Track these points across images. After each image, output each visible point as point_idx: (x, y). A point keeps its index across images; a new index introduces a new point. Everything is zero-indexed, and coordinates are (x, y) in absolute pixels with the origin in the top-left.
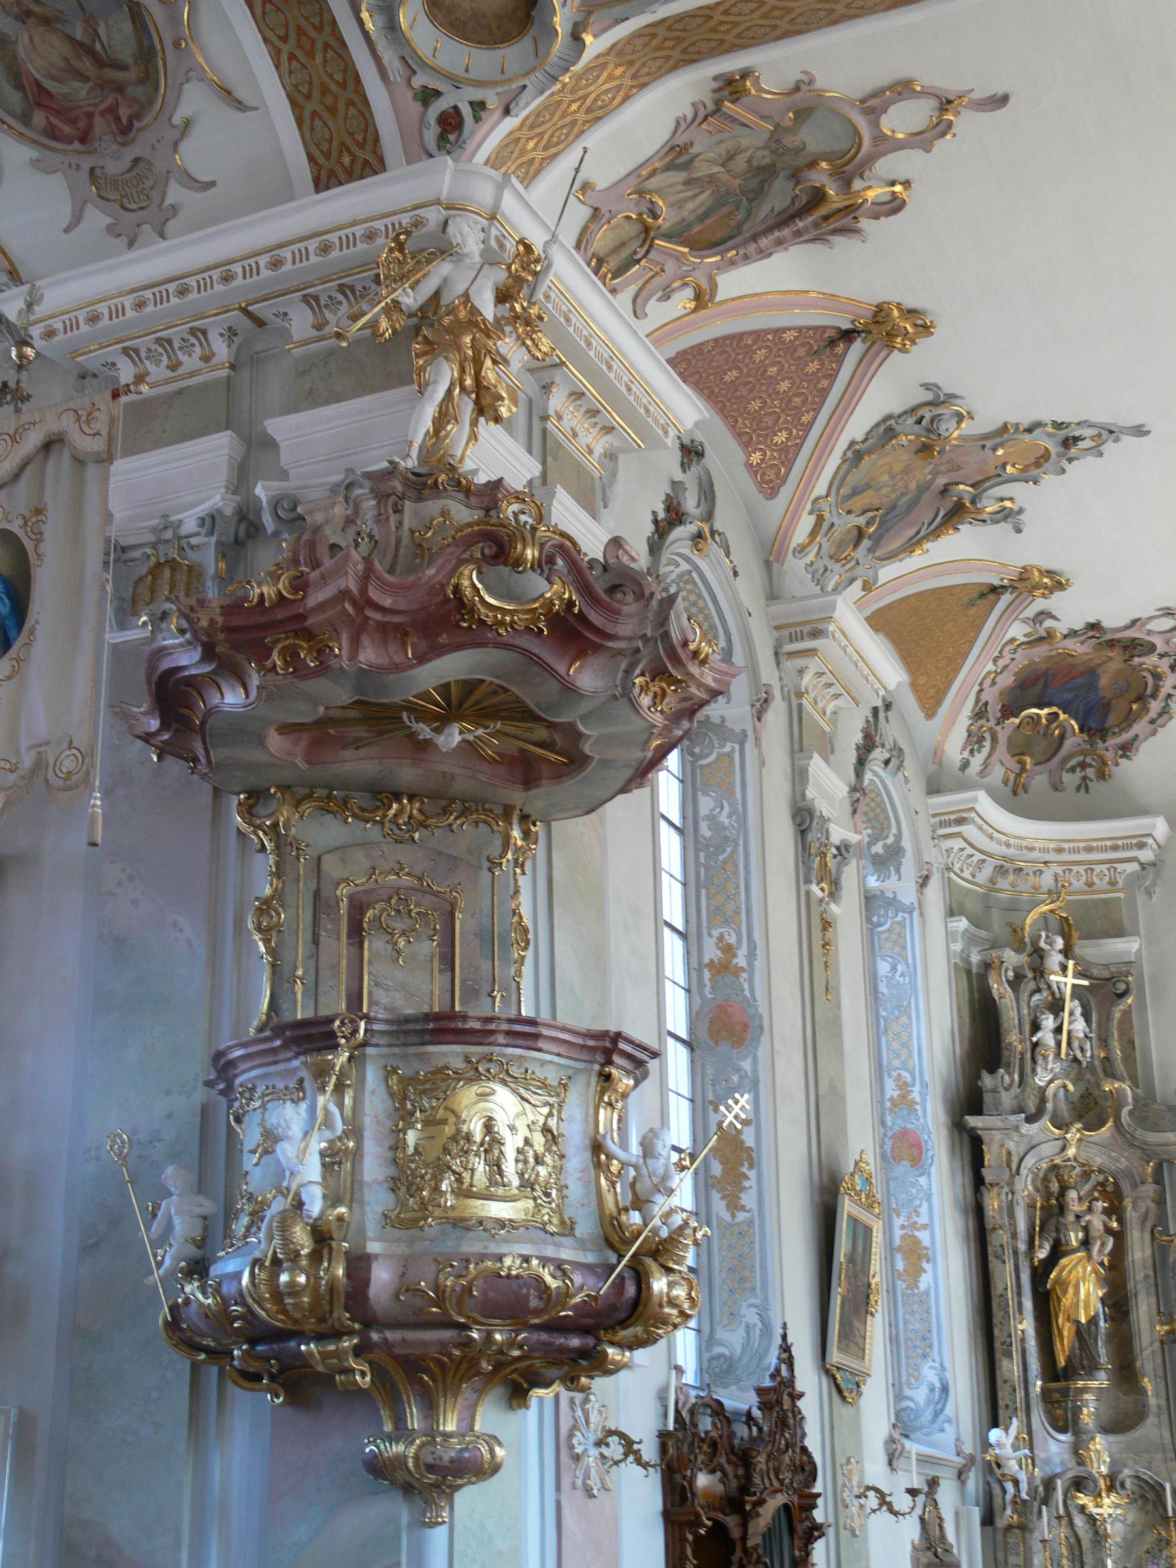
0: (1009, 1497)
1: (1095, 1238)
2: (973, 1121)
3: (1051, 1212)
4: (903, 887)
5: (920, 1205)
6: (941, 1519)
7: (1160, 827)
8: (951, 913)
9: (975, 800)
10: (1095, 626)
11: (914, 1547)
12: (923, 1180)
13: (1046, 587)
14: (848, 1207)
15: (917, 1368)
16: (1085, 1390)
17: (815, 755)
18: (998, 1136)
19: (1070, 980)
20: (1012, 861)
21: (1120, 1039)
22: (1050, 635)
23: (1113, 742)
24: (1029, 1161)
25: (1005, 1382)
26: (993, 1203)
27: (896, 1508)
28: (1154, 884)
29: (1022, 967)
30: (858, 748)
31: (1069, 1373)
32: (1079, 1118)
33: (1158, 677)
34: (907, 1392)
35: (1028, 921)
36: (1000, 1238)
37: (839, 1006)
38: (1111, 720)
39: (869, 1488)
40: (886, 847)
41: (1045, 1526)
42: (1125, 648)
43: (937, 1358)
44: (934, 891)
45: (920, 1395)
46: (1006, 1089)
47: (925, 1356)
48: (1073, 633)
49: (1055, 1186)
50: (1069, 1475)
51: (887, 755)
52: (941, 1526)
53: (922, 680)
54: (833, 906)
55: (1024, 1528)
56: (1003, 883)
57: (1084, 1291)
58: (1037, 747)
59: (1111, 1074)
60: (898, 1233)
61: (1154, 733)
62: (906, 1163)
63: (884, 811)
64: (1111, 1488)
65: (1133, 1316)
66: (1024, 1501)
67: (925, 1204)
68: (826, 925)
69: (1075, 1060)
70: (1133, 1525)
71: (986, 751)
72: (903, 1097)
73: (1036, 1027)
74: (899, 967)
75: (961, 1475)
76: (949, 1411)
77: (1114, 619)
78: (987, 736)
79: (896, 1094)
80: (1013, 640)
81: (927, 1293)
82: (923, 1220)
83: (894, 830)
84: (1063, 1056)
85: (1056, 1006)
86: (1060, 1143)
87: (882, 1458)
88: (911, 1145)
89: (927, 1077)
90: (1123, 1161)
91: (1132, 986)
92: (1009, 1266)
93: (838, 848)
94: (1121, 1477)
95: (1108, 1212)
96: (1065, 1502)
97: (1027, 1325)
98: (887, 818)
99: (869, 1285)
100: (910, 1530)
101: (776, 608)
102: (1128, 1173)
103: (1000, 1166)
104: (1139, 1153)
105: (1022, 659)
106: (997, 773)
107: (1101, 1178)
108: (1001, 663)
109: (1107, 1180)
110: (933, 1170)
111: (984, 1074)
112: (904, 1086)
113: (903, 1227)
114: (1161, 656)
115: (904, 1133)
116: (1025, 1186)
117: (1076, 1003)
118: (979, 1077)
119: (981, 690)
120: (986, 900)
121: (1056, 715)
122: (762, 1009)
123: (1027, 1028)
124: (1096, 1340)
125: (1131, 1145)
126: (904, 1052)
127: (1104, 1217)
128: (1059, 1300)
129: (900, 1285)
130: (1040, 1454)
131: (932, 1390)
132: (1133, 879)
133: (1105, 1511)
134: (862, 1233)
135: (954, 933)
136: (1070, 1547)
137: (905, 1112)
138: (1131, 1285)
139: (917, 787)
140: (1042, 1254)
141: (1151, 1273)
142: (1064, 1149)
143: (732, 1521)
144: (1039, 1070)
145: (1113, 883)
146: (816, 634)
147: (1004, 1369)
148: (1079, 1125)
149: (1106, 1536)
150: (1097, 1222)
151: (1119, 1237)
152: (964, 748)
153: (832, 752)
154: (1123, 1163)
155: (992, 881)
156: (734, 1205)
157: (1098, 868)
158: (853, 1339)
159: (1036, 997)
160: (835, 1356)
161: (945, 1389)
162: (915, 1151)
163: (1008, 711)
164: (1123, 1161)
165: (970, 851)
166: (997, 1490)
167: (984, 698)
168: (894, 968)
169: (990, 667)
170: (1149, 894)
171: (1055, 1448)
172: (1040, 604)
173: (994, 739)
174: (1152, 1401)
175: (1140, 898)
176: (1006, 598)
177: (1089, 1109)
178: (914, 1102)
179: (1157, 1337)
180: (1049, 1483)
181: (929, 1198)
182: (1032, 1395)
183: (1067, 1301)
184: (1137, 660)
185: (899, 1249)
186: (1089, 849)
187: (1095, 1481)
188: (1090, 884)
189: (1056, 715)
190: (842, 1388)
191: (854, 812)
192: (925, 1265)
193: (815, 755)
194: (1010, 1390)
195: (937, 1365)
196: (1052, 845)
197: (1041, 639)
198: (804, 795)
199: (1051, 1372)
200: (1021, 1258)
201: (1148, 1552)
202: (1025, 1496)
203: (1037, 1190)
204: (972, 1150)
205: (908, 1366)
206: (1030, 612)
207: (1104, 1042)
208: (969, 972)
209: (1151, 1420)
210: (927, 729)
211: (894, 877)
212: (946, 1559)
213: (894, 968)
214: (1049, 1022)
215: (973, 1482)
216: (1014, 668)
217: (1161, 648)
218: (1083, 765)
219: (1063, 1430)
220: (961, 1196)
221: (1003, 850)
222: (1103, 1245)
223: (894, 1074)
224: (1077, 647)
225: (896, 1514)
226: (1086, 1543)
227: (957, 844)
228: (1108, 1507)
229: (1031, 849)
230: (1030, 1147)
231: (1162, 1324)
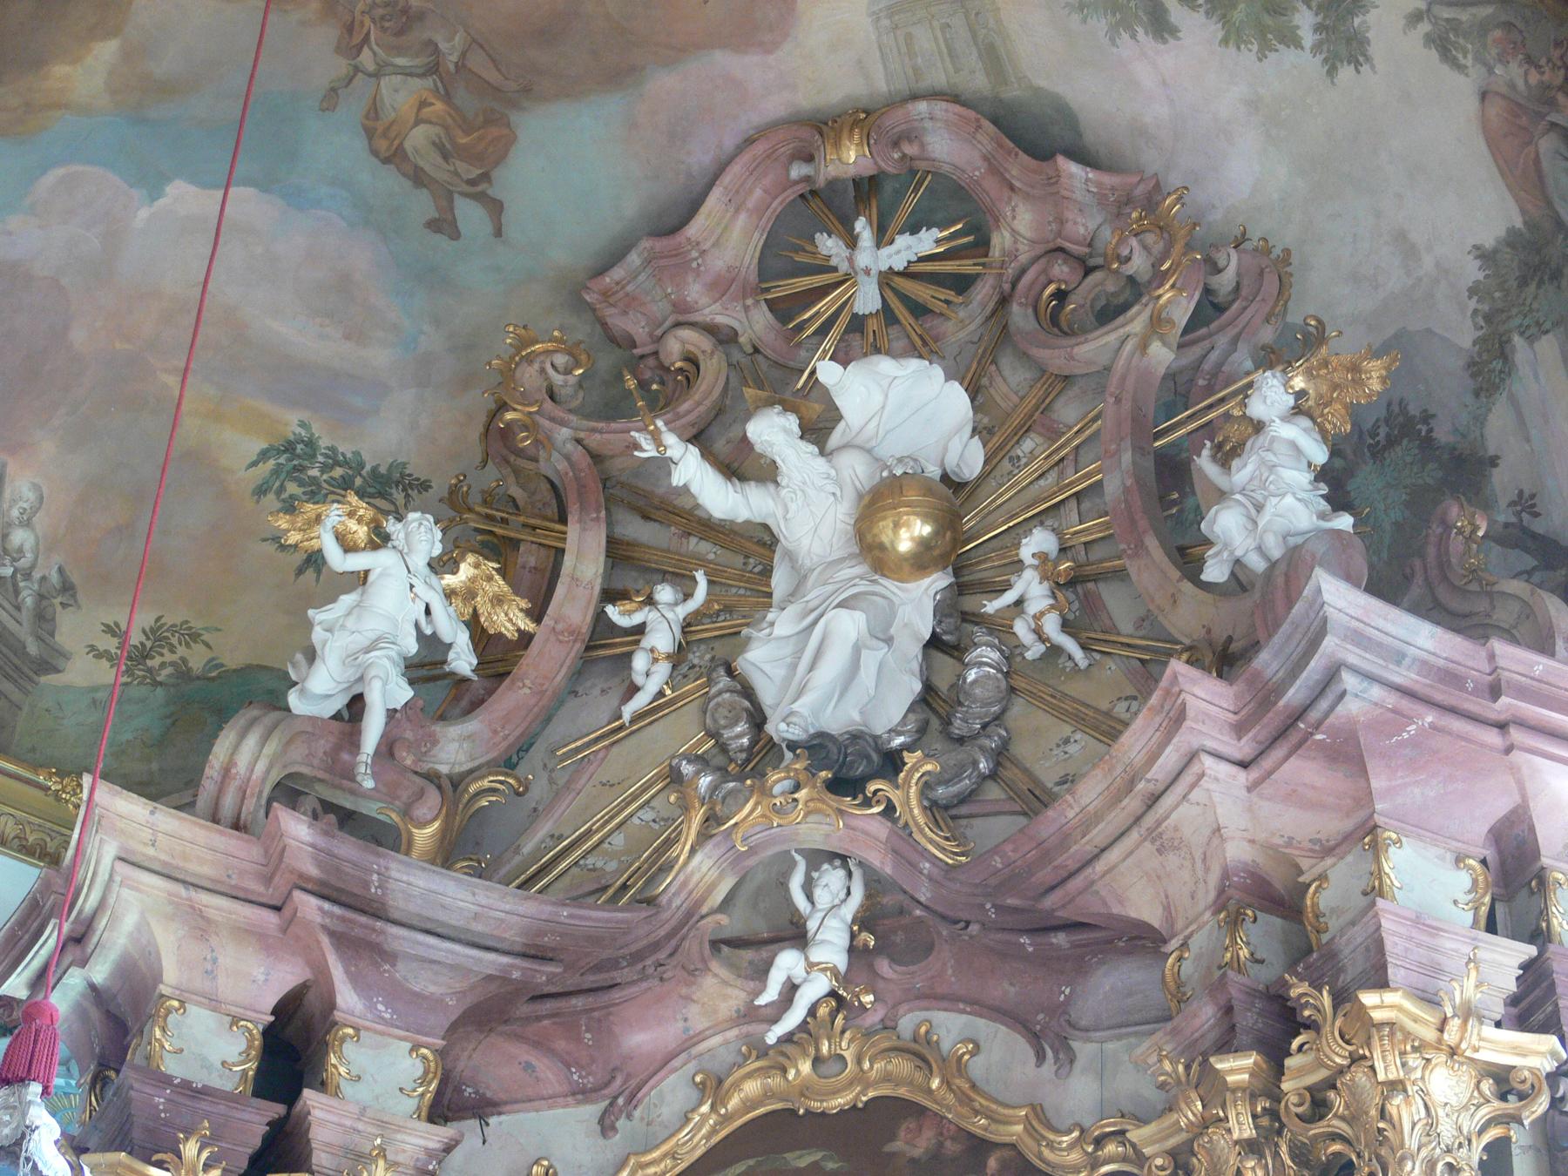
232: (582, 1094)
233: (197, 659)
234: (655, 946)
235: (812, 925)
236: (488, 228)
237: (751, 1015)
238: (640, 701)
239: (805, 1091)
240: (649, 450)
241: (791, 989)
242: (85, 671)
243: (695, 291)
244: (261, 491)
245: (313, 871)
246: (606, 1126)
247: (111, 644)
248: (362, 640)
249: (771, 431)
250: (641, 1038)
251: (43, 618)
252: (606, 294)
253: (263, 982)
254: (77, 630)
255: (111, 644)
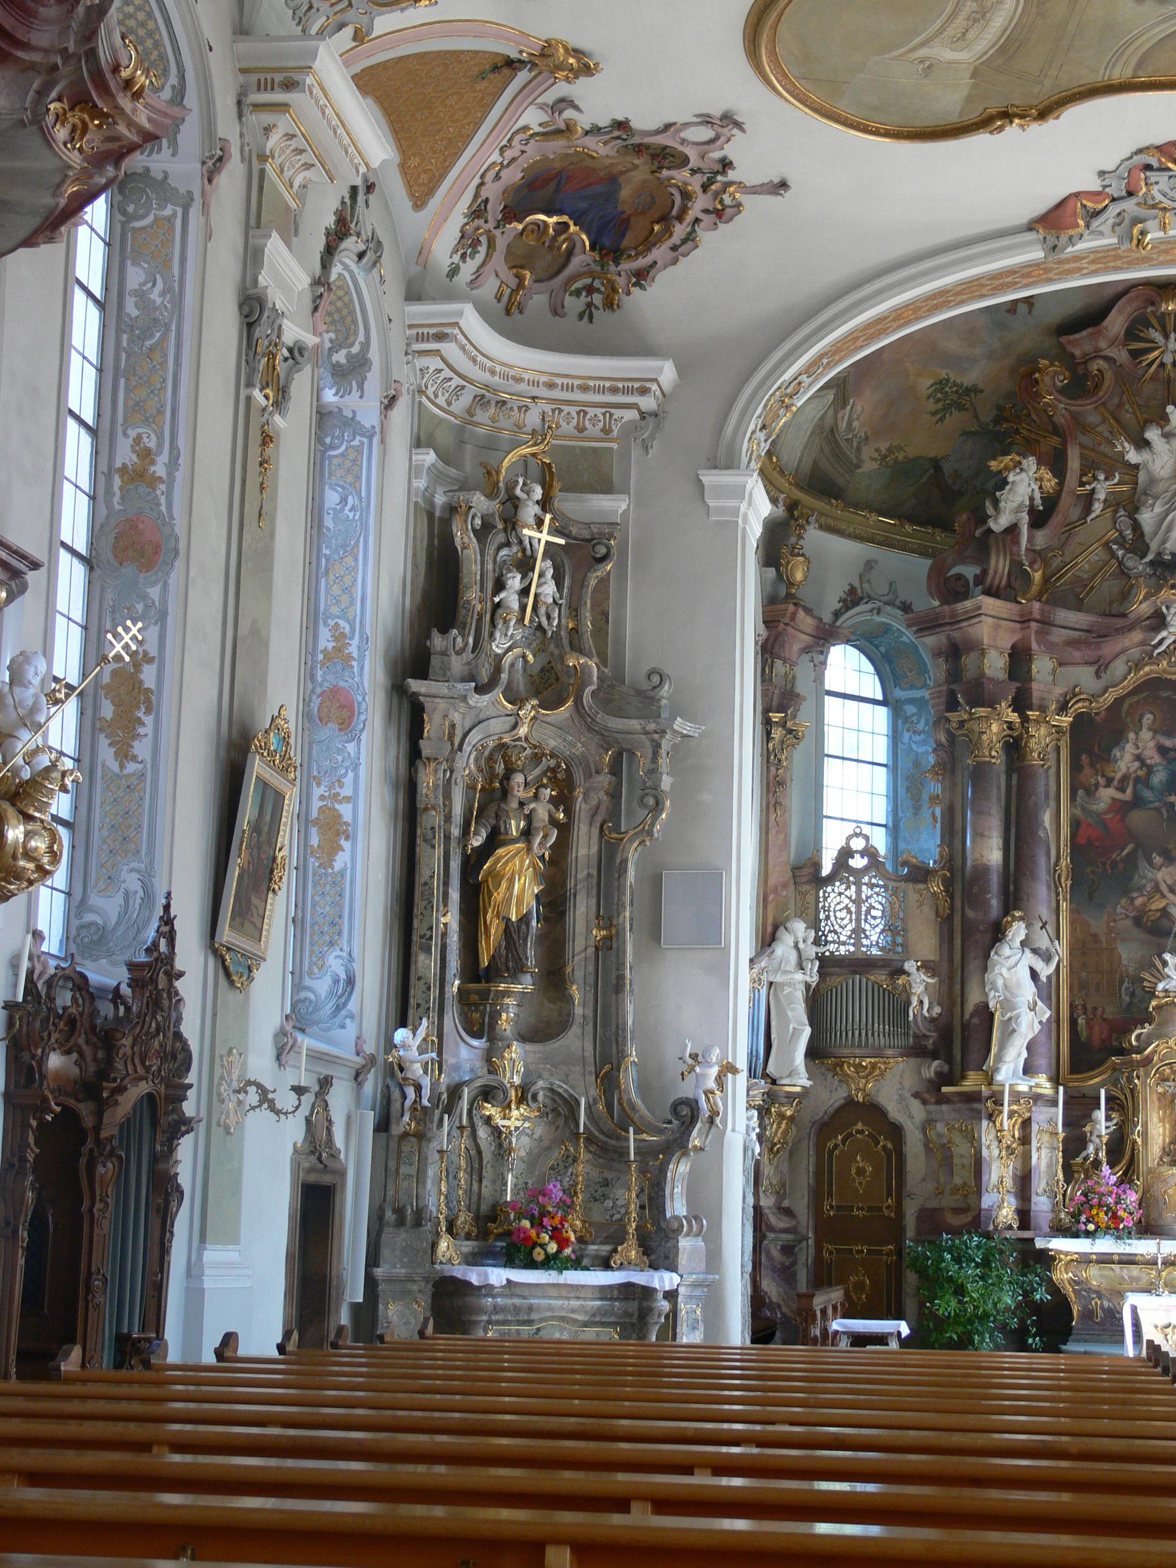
0: (408, 1103)
1: (537, 829)
2: (415, 685)
3: (492, 797)
4: (365, 406)
5: (346, 774)
6: (330, 1122)
7: (667, 373)
8: (418, 443)
9: (460, 313)
10: (622, 125)
11: (296, 1150)
12: (351, 747)
13: (571, 70)
14: (257, 768)
15: (322, 956)
16: (507, 993)
17: (274, 234)
18: (442, 704)
19: (545, 537)
20: (495, 391)
21: (593, 609)
22: (568, 130)
23: (626, 266)
24: (474, 737)
25: (420, 978)
26: (428, 780)
27: (279, 1106)
28: (652, 437)
29: (492, 515)
30: (328, 234)
31: (493, 973)
32: (537, 694)
33: (686, 196)
34: (308, 982)
35: (506, 464)
36: (432, 819)
37: (272, 536)
38: (626, 242)
39: (250, 1083)
40: (349, 357)
41: (444, 1136)
42: (654, 156)
43: (345, 948)
44: (401, 416)
45: (322, 986)
46: (458, 653)
47: (332, 944)
48: (595, 130)
49: (500, 768)
50: (478, 1083)
51: (362, 247)
52: (329, 1130)
53: (413, 162)
54: (277, 418)
55: (421, 1136)
56: (482, 416)
57: (518, 886)
58: (537, 261)
59: (577, 648)
60: (316, 804)
61: (675, 262)
62: (333, 726)
63: (352, 313)
64: (521, 1100)
65: (569, 918)
66: (425, 1108)
67: (351, 775)
68: (267, 439)
69: (540, 627)
70: (541, 1139)
71: (480, 258)
72: (338, 650)
73: (500, 586)
74: (350, 499)
75: (358, 1076)
76: (352, 1006)
77: (645, 120)
78: (483, 239)
79: (330, 645)
80: (525, 128)
81: (342, 873)
82: (347, 791)
83: (361, 337)
84: (527, 622)
85: (525, 565)
86: (512, 720)
87: (269, 1050)
88: (342, 706)
89: (368, 631)
90: (578, 746)
91: (614, 551)
92: (439, 852)
93: (290, 350)
94: (533, 1089)
95: (554, 802)
96: (470, 1111)
97: (451, 919)
98: (355, 322)
99: (274, 859)
100: (293, 1131)
101: (244, 46)
102: (584, 761)
103: (441, 739)
104: (597, 739)
105: (534, 152)
106: (490, 286)
107: (553, 763)
108: (509, 154)
109: (559, 766)
110: (364, 737)
111: (435, 632)
112: (340, 638)
113: (322, 798)
114: (694, 172)
115: (335, 691)
116: (467, 764)
117: (549, 563)
118: (429, 637)
119: (482, 184)
120: (461, 434)
121: (565, 226)
122: (180, 529)
123: (490, 586)
124: (525, 940)
125: (590, 729)
126: (345, 599)
127: (552, 807)
128: (490, 895)
129: (313, 863)
130: (449, 1059)
131: (336, 981)
132: (631, 429)
133: (512, 1123)
134: (272, 800)
135: (419, 467)
136: (470, 1159)
137: (339, 668)
138: (571, 883)
139: (394, 290)
140: (477, 842)
141: (595, 873)
142: (515, 726)
143: (85, 1109)
144: (498, 635)
145: (606, 431)
146: (289, 85)
147: (420, 965)
148: (535, 702)
149: (510, 1150)
150: (542, 811)
151: (565, 830)
152: (455, 251)
153: (296, 234)
154: (579, 749)
155: (470, 412)
156: (124, 754)
157: (591, 412)
158: (249, 916)
159: (504, 552)
160: (226, 935)
161: (351, 981)
162: (345, 714)
163: (511, 213)
164: (578, 746)
165: (447, 373)
166: (396, 1094)
167: (484, 194)
168: (344, 500)
169: (495, 157)
170: (646, 448)
171: (466, 1053)
172: (561, 89)
173: (491, 245)
174: (578, 1011)
175: (635, 452)
176: (523, 76)
177: (549, 685)
178: (350, 657)
179: (592, 942)
180: (455, 1092)
181: (356, 767)
182: (448, 995)
183: (499, 895)
184: (665, 173)
185: (316, 822)
186: (585, 389)
187: (505, 1092)
188: (581, 429)
189: (565, 226)
190: (232, 969)
191: (316, 309)
192: (343, 842)
193: (274, 234)
194: (424, 989)
195: (344, 954)
196: (543, 379)
197: (558, 132)
198: (255, 282)
199: (472, 971)
200: (453, 844)
201: (552, 1168)
202: (425, 1102)
203: (480, 770)
204: (411, 718)
205: (312, 952)
206: (550, 97)
207: (574, 611)
208: (431, 515)
209: (575, 1030)
210: (413, 222)
211: (355, 394)
212: (331, 1164)
213: (344, 500)
214: (515, 582)
215: (371, 1085)
216: (523, 162)
217: (694, 162)
218: (590, 290)
219: (477, 1035)
220: (393, 768)
221: (486, 377)
222: (545, 837)
223: (331, 623)
224: (598, 148)
225: (278, 1112)
226: (487, 1156)
227: (434, 363)
228: (516, 1120)
229: (519, 380)
230: (478, 720)
231: (599, 928)
232: (1087, 663)
233: (901, 456)
234: (1124, 627)
235: (1169, 619)
236: (1027, 311)
237: (1144, 643)
238: (1093, 516)
239: (1164, 671)
240: (1119, 448)
241: (1163, 639)
242: (869, 466)
243: (1103, 344)
244: (929, 397)
245: (1038, 617)
246: (1098, 675)
247: (876, 455)
248: (1015, 505)
249: (1153, 434)
250: (1109, 648)
251: (859, 450)
252: (1069, 342)
253: (1007, 640)
254: (867, 452)
255: (876, 455)
